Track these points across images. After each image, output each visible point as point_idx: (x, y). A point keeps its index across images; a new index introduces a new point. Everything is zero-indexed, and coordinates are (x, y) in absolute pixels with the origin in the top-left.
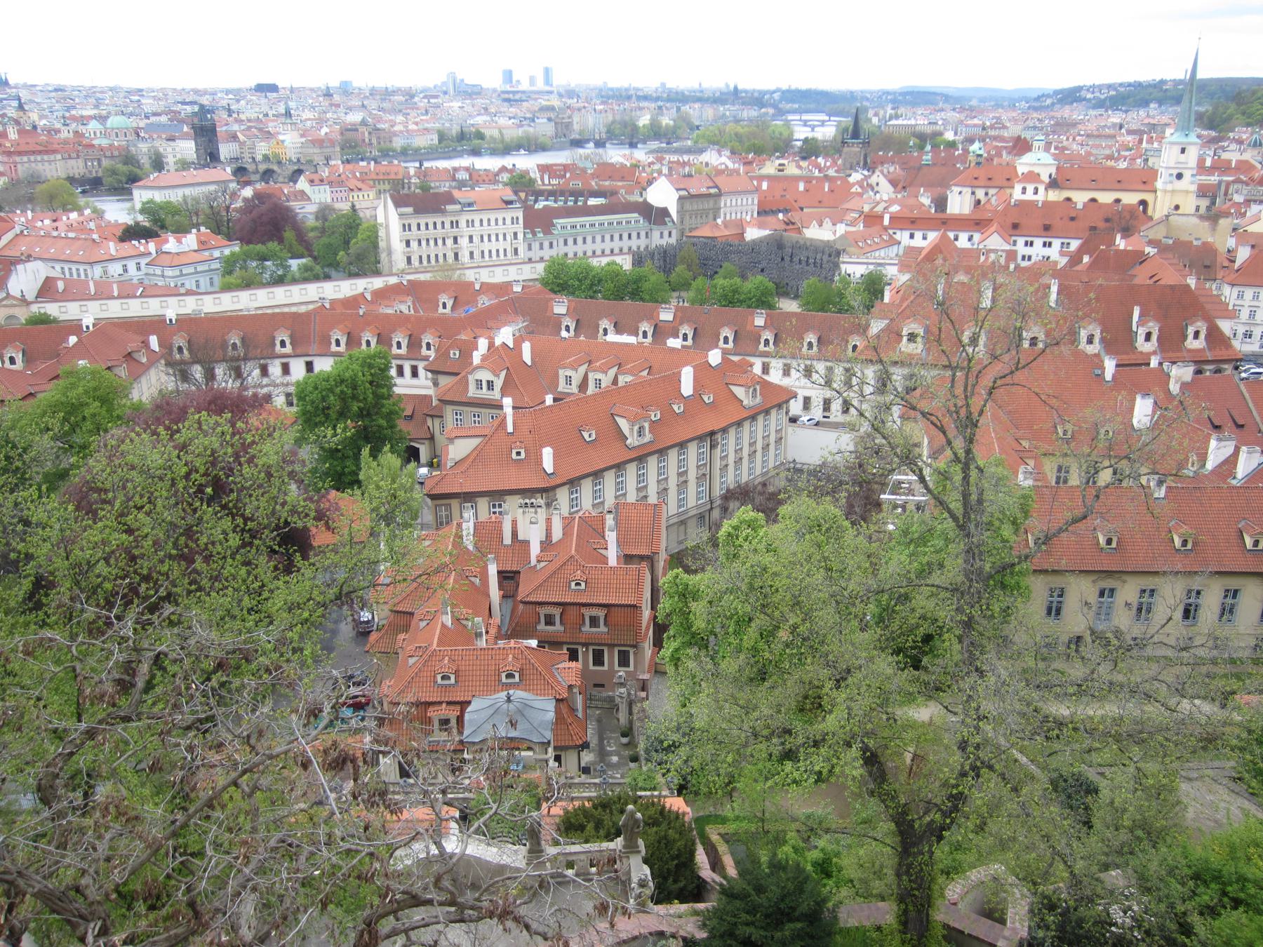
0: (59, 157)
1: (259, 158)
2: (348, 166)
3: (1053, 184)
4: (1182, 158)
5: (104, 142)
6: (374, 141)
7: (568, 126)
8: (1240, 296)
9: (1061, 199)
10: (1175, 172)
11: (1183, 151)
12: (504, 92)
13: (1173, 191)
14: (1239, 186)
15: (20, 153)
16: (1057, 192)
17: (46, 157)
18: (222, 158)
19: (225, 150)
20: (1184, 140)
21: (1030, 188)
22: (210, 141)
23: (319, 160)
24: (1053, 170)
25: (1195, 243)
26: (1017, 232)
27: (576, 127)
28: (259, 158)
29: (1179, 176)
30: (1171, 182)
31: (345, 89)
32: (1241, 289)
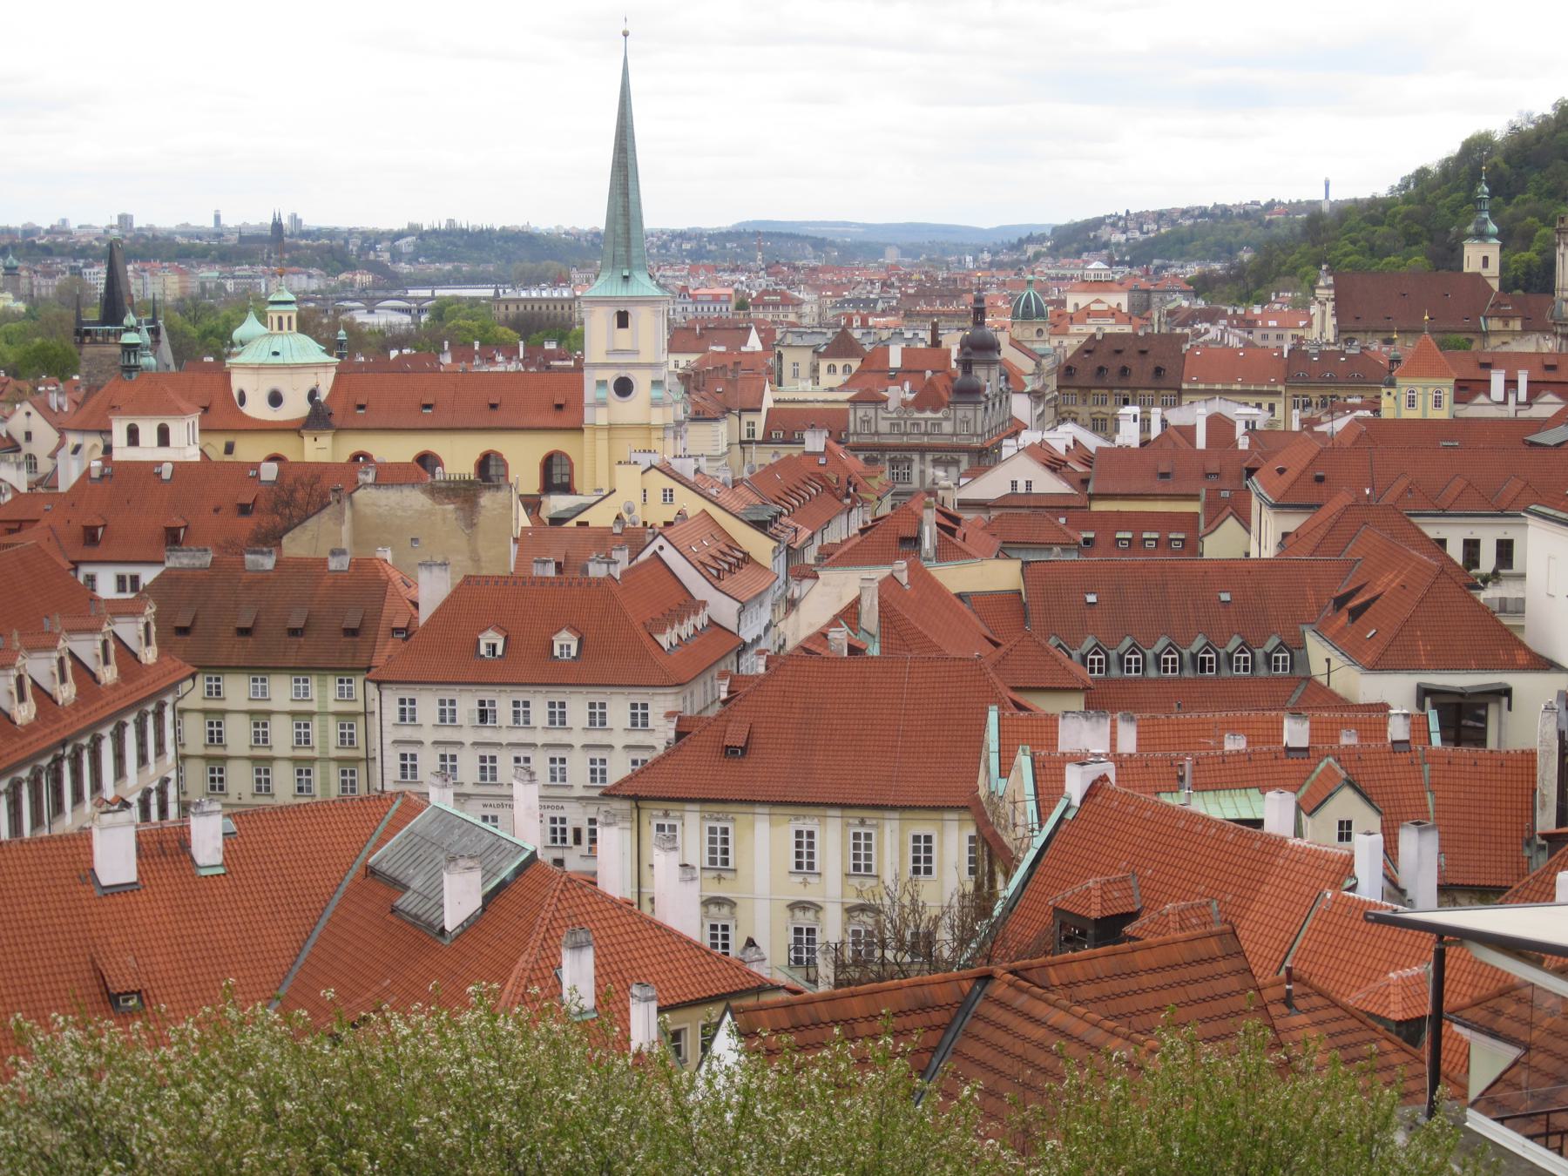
3: (319, 418)
4: (623, 338)
8: (407, 714)
9: (344, 458)
10: (611, 376)
11: (623, 320)
13: (611, 428)
14: (871, 413)
16: (326, 440)
20: (620, 291)
21: (148, 431)
24: (325, 383)
25: (334, 564)
26: (96, 553)
29: (624, 387)
30: (602, 404)
32: (407, 694)
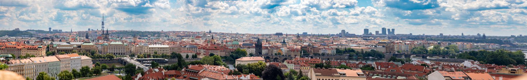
0: (219, 51)
1: (274, 54)
2: (302, 59)
5: (231, 48)
6: (312, 51)
7: (393, 49)
12: (364, 37)
15: (210, 50)
17: (216, 51)
18: (263, 53)
19: (264, 52)
22: (260, 49)
23: (293, 56)
27: (396, 49)
28: (274, 54)
31: (305, 34)
